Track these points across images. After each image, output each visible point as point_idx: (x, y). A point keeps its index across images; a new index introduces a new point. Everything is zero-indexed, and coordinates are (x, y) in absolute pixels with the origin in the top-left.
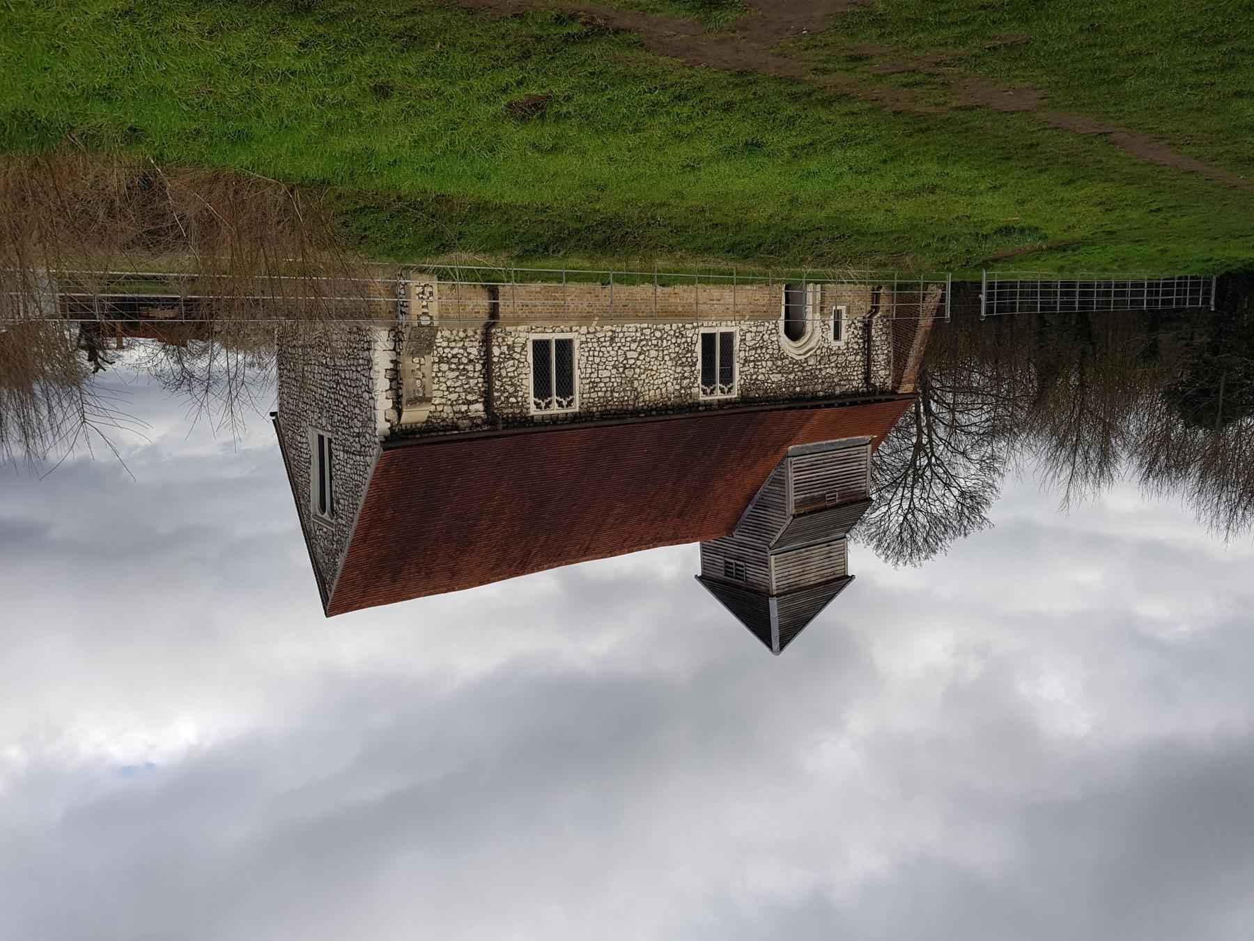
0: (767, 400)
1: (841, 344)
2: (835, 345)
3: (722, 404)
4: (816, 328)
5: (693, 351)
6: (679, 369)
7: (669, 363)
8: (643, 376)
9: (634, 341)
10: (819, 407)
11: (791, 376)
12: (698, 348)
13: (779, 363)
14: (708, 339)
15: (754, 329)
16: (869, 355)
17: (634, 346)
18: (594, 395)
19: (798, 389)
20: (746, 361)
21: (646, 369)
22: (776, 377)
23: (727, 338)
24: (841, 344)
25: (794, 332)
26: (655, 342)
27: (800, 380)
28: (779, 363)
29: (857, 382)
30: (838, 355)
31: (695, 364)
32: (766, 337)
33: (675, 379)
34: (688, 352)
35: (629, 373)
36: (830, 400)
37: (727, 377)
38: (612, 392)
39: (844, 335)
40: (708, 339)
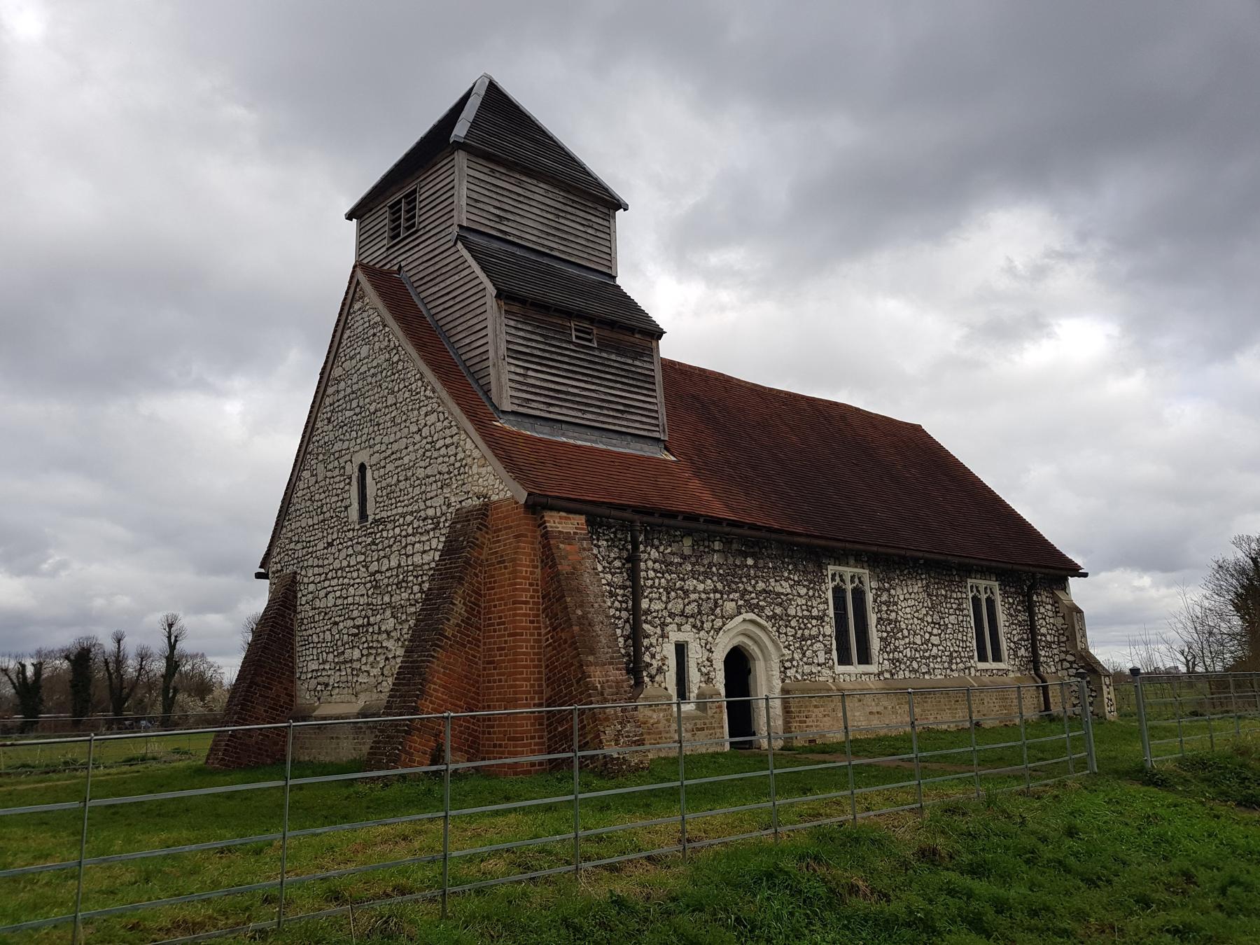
1: (675, 636)
4: (708, 659)
5: (881, 639)
7: (903, 626)
9: (935, 657)
11: (761, 585)
12: (875, 644)
13: (778, 610)
22: (785, 588)
24: (675, 636)
28: (778, 610)
29: (650, 557)
30: (682, 614)
31: (879, 619)
33: (896, 604)
37: (839, 593)
38: (946, 597)
39: (669, 651)
40: (865, 658)
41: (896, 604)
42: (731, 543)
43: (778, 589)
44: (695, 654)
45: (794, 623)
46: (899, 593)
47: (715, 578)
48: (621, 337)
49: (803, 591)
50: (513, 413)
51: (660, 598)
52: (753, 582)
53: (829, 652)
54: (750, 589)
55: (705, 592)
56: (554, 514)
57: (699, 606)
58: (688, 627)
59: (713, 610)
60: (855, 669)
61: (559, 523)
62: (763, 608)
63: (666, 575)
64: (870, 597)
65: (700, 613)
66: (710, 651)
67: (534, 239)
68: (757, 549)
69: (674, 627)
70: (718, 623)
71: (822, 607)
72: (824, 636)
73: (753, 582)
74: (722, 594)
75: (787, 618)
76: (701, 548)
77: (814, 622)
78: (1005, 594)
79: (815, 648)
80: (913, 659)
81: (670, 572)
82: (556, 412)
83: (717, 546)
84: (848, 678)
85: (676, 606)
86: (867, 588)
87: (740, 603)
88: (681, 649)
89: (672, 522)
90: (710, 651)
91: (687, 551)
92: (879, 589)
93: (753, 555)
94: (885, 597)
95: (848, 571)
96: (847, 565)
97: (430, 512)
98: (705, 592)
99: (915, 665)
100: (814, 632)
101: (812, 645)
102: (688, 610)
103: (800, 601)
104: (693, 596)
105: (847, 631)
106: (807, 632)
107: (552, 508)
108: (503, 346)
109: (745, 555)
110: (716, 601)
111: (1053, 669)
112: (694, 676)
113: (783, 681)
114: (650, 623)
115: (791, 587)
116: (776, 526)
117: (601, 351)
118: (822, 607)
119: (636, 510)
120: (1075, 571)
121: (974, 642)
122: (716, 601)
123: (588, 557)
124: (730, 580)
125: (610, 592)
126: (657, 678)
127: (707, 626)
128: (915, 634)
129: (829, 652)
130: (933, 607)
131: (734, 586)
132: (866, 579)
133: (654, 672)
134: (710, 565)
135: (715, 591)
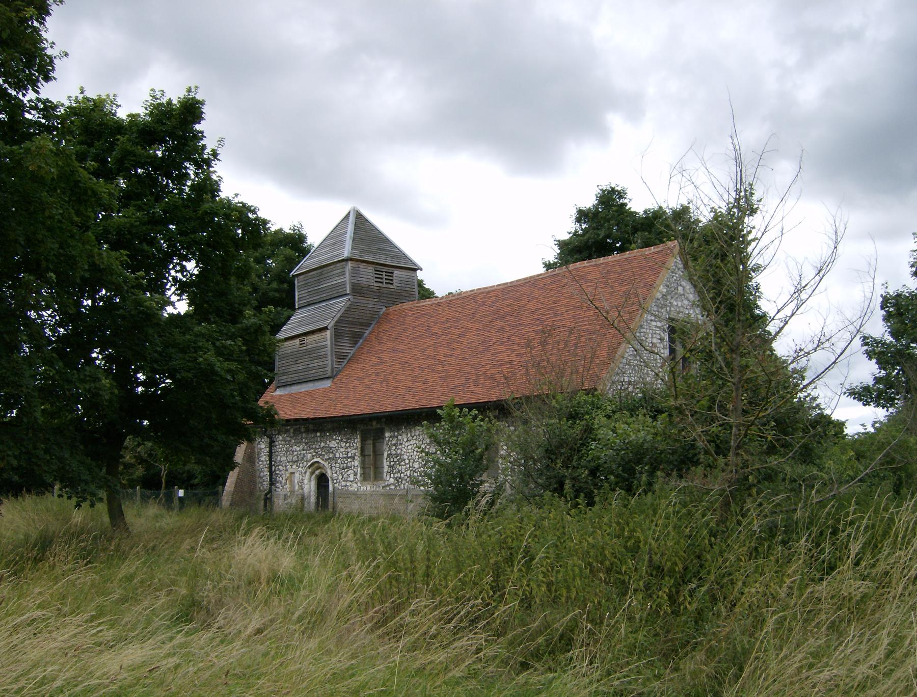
5: (390, 466)
6: (399, 451)
7: (405, 457)
11: (323, 444)
13: (331, 456)
15: (348, 484)
16: (271, 460)
19: (318, 434)
22: (333, 444)
25: (322, 481)
28: (331, 456)
31: (389, 455)
32: (340, 477)
33: (401, 444)
34: (392, 466)
59: (303, 459)
75: (334, 459)
85: (290, 458)
100: (349, 465)
103: (342, 450)
109: (317, 431)
129: (355, 474)
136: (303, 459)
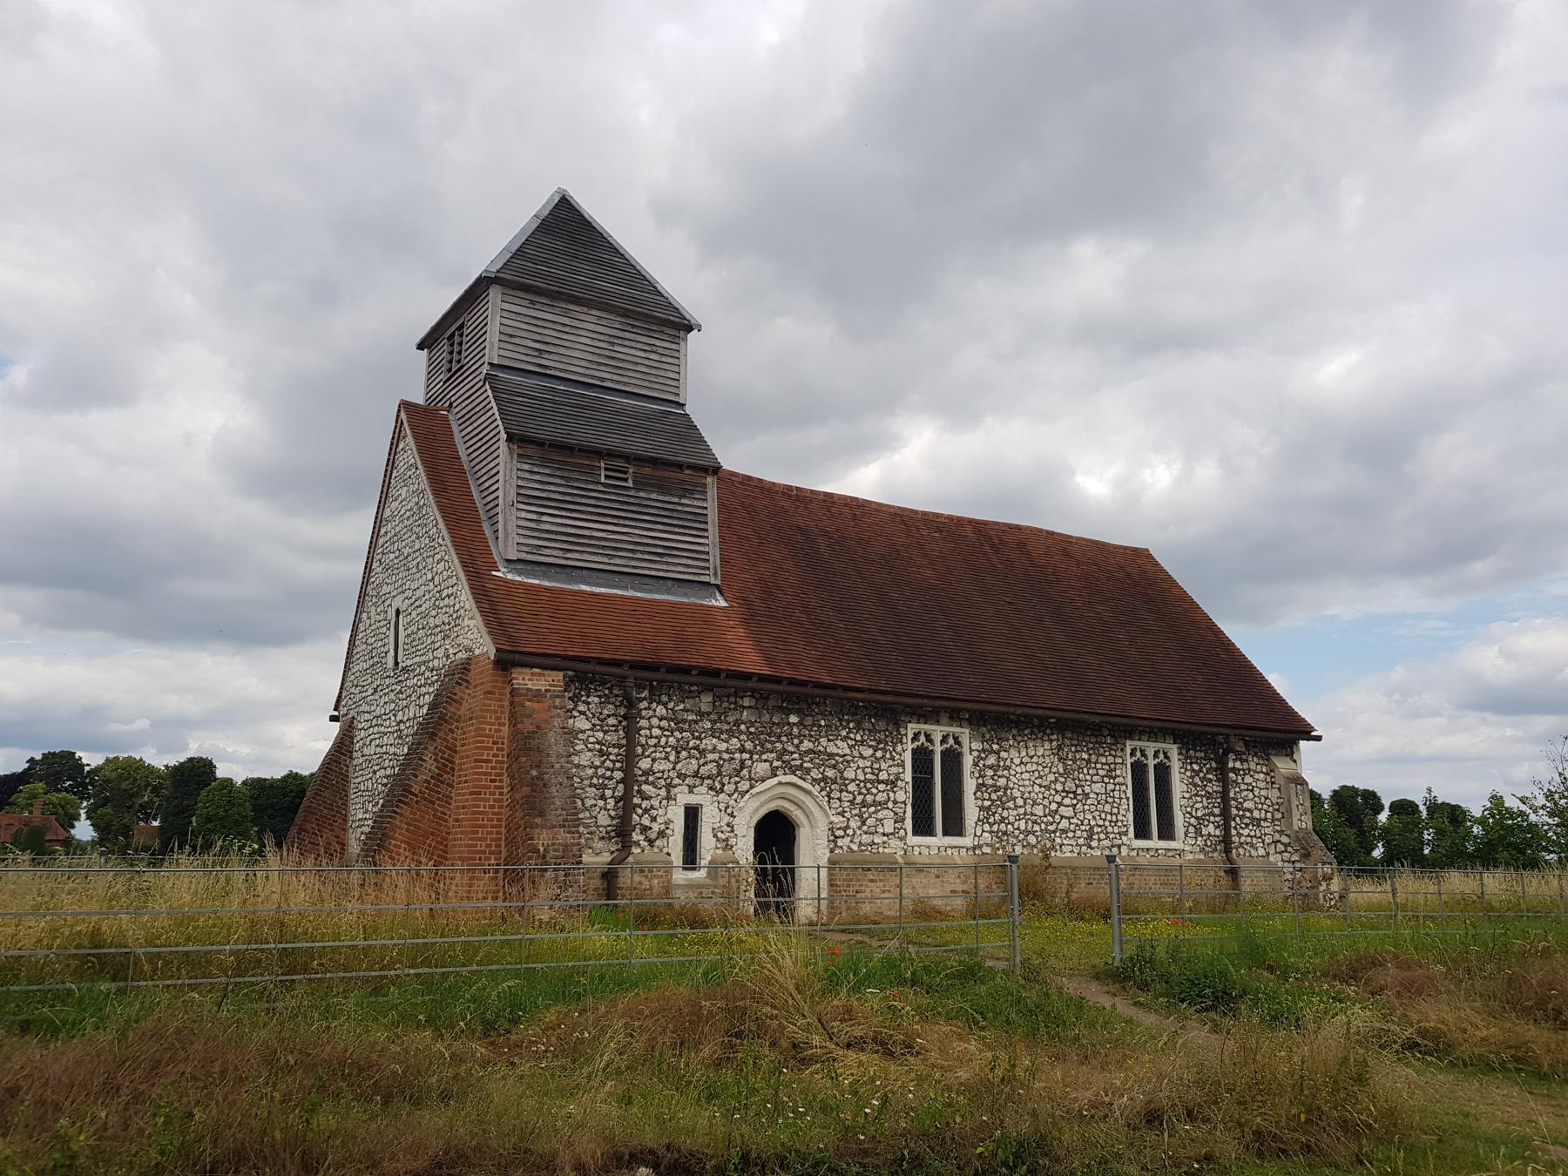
0: (854, 709)
1: (684, 798)
2: (702, 797)
3: (930, 715)
4: (731, 828)
5: (981, 808)
6: (1002, 782)
7: (1016, 793)
8: (1051, 777)
9: (1064, 831)
10: (763, 678)
11: (807, 745)
12: (971, 812)
13: (830, 773)
14: (954, 825)
17: (1064, 824)
18: (1111, 760)
19: (793, 719)
20: (892, 784)
21: (1048, 788)
22: (841, 747)
23: (923, 826)
24: (684, 798)
26: (1037, 828)
27: (790, 735)
28: (830, 773)
31: (979, 787)
32: (854, 824)
33: (1008, 768)
34: (989, 808)
35: (1070, 785)
36: (723, 685)
38: (1088, 761)
39: (677, 815)
41: (1008, 768)
42: (767, 698)
43: (832, 749)
44: (710, 818)
45: (852, 787)
46: (1013, 756)
47: (743, 737)
48: (666, 474)
49: (868, 752)
50: (519, 561)
51: (667, 758)
52: (796, 741)
53: (900, 820)
54: (791, 749)
55: (727, 751)
56: (519, 669)
57: (719, 766)
58: (703, 789)
59: (738, 772)
60: (938, 840)
61: (526, 679)
62: (808, 771)
63: (677, 734)
64: (968, 761)
65: (719, 773)
66: (732, 815)
67: (581, 370)
68: (804, 706)
69: (686, 789)
70: (744, 786)
71: (894, 770)
72: (895, 802)
73: (796, 741)
74: (751, 753)
76: (725, 705)
77: (882, 787)
78: (1186, 758)
79: (880, 815)
80: (1028, 832)
81: (682, 731)
82: (574, 559)
83: (746, 702)
84: (925, 851)
86: (966, 750)
87: (776, 764)
88: (692, 814)
89: (684, 678)
90: (732, 815)
91: (705, 708)
92: (984, 750)
93: (798, 712)
94: (991, 760)
95: (938, 731)
96: (938, 722)
97: (436, 663)
98: (727, 751)
99: (1032, 839)
100: (881, 797)
101: (876, 812)
102: (704, 771)
103: (861, 763)
104: (710, 756)
105: (931, 799)
106: (869, 798)
107: (523, 665)
108: (513, 492)
109: (789, 712)
110: (742, 762)
111: (1261, 852)
112: (708, 846)
113: (832, 851)
114: (653, 784)
115: (850, 747)
116: (827, 679)
117: (639, 490)
118: (894, 770)
119: (635, 666)
120: (1306, 733)
121: (1131, 816)
122: (742, 762)
123: (559, 716)
124: (762, 740)
125: (600, 751)
126: (658, 843)
127: (729, 788)
128: (1035, 803)
129: (900, 820)
130: (1066, 773)
131: (769, 746)
132: (965, 739)
133: (653, 836)
134: (737, 723)
135: (742, 750)
136: (738, 772)
